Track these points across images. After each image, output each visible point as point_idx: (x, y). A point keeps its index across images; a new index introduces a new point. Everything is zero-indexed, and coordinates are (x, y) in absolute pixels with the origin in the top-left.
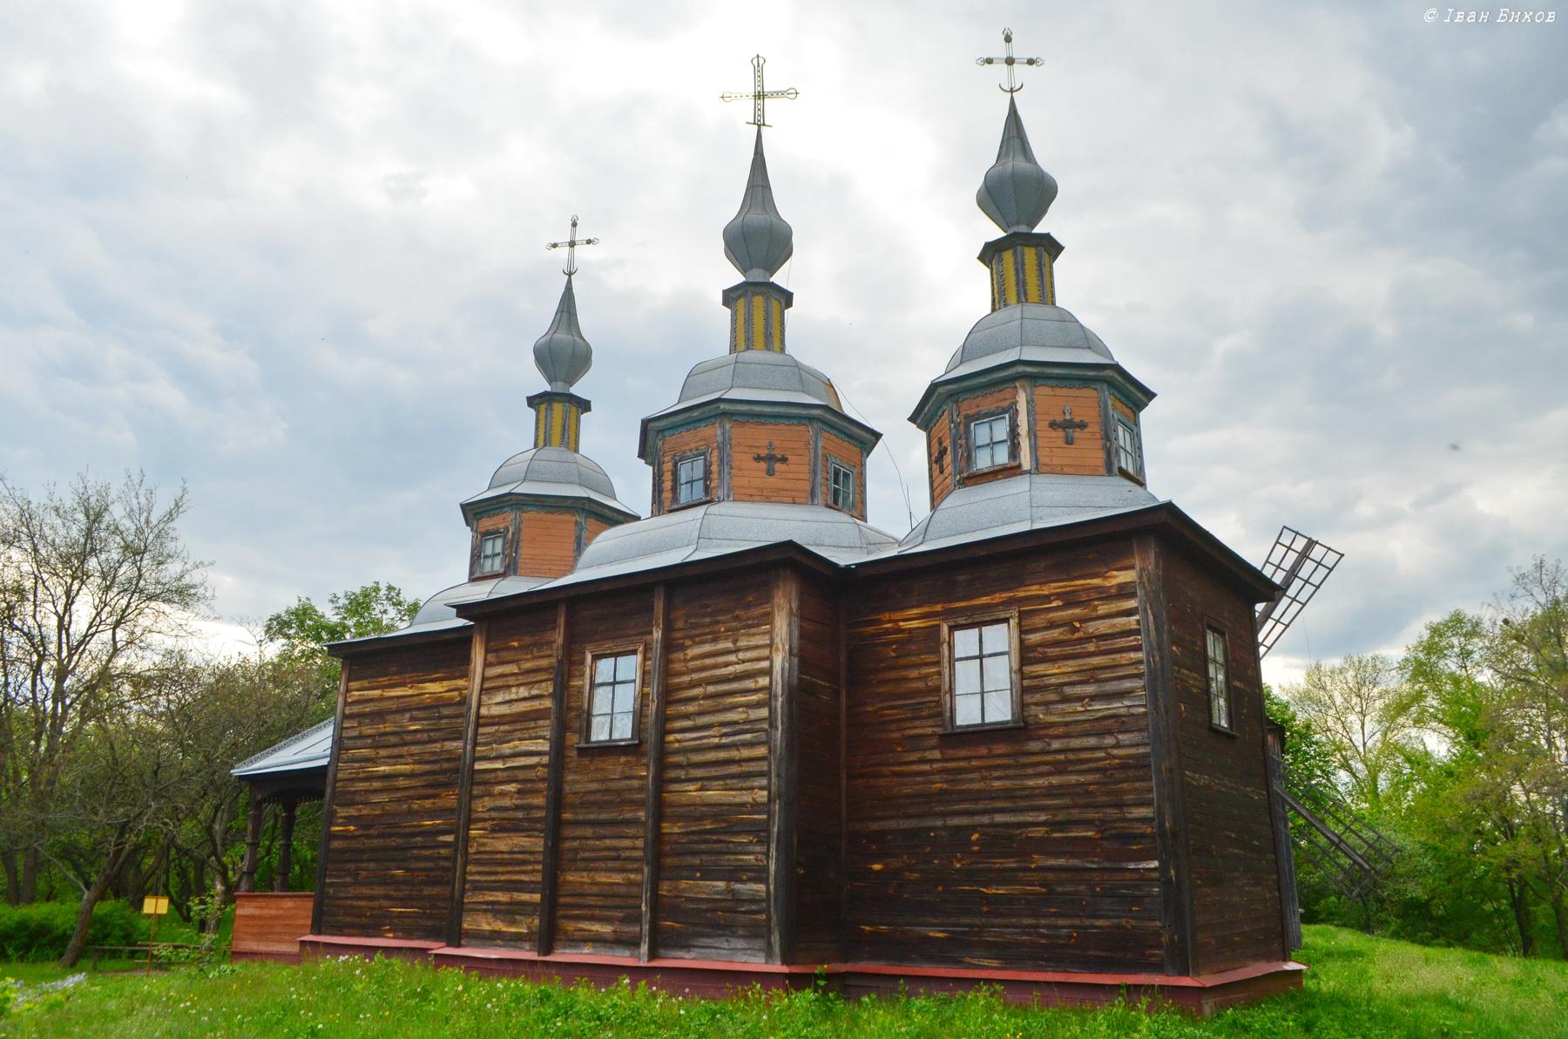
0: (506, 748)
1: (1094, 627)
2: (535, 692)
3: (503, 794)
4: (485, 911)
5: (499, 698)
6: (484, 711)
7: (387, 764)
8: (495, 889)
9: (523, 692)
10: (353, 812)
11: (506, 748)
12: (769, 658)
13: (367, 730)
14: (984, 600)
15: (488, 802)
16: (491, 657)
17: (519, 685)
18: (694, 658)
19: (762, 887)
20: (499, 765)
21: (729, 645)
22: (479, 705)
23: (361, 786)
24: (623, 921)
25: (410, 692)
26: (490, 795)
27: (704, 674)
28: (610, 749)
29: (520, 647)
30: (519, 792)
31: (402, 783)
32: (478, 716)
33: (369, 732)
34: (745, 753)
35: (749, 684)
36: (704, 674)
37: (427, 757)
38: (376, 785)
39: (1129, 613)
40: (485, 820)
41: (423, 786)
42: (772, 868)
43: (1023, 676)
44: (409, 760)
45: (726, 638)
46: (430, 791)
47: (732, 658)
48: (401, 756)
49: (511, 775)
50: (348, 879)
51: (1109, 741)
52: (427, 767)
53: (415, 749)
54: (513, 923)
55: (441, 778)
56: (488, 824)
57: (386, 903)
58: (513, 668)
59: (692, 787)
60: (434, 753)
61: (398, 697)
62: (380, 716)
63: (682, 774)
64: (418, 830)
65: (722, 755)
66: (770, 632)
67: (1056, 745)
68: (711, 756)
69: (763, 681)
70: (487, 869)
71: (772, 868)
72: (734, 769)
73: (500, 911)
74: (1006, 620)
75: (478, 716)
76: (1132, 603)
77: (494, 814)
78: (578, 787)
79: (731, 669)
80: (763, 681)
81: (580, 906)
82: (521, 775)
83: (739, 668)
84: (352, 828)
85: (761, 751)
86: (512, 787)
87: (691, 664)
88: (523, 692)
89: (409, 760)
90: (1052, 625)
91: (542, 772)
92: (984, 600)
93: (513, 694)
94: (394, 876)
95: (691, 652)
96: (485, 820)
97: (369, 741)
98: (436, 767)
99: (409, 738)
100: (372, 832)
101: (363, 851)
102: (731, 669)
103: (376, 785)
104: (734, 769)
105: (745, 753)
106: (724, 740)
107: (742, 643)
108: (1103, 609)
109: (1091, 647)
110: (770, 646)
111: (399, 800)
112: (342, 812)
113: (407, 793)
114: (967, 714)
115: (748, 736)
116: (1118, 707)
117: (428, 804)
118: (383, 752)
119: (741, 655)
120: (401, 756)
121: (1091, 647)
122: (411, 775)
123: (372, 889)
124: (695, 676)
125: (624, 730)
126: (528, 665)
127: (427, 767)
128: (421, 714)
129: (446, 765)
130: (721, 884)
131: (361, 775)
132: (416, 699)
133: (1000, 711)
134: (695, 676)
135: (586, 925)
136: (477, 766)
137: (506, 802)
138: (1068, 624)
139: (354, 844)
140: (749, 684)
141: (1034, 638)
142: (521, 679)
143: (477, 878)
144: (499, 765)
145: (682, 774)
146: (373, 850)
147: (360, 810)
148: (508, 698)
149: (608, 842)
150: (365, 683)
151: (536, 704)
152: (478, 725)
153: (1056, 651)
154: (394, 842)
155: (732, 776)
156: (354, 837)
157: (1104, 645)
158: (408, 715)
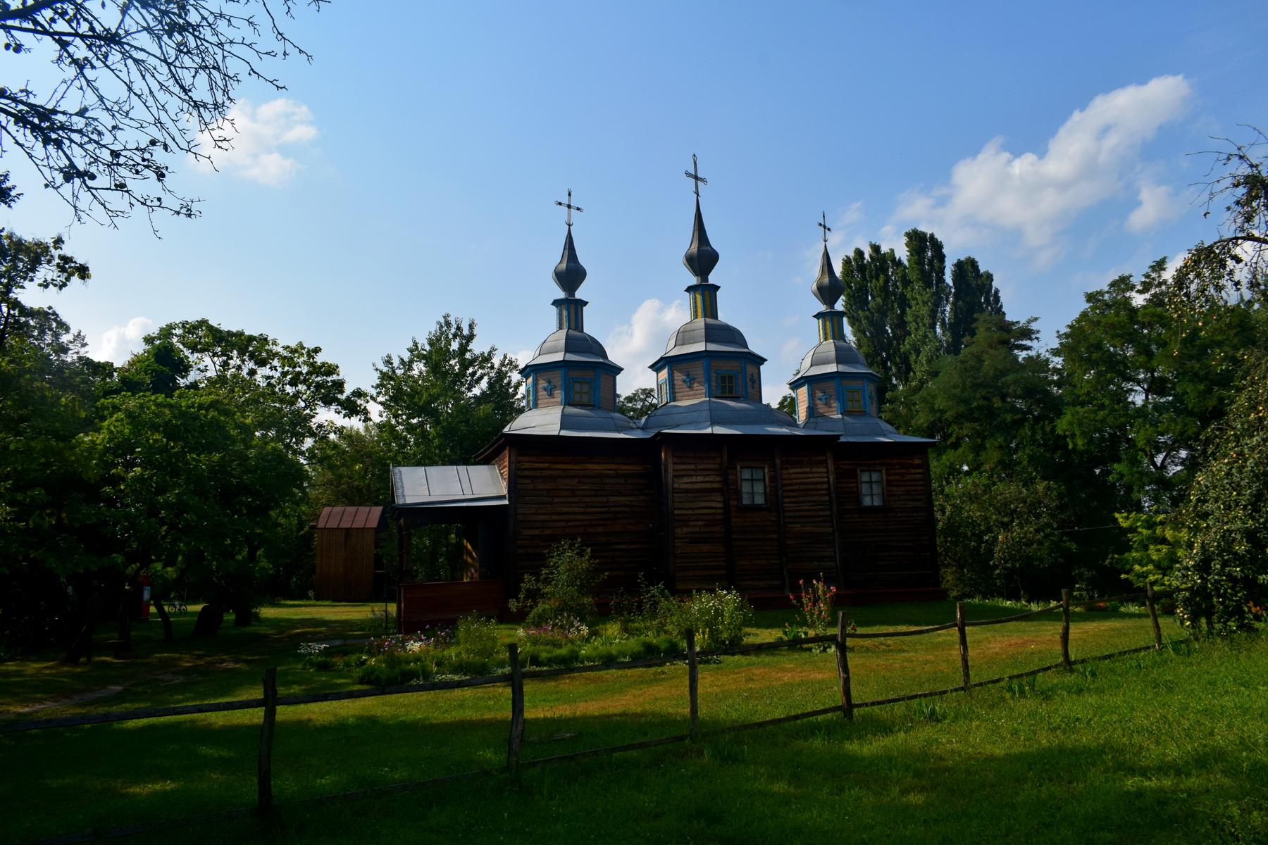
0: (694, 505)
1: (908, 477)
2: (706, 479)
3: (696, 526)
5: (686, 480)
6: (676, 486)
9: (699, 479)
10: (535, 532)
12: (828, 477)
15: (685, 530)
16: (676, 460)
17: (697, 475)
18: (793, 473)
19: (834, 564)
20: (691, 512)
21: (808, 470)
22: (673, 483)
25: (576, 467)
27: (798, 481)
28: (754, 508)
30: (704, 525)
32: (673, 489)
34: (821, 513)
35: (819, 486)
36: (798, 481)
38: (554, 517)
39: (920, 473)
40: (684, 538)
42: (838, 557)
44: (582, 505)
45: (807, 467)
47: (811, 475)
51: (916, 514)
52: (598, 510)
58: (692, 467)
59: (798, 526)
61: (565, 470)
63: (792, 520)
65: (812, 513)
66: (827, 467)
68: (806, 513)
71: (838, 557)
72: (817, 519)
74: (881, 471)
75: (673, 489)
76: (921, 471)
79: (810, 480)
80: (825, 486)
83: (814, 480)
85: (828, 513)
86: (701, 523)
87: (792, 476)
88: (699, 479)
89: (582, 505)
90: (896, 474)
91: (718, 517)
93: (694, 479)
95: (791, 471)
96: (684, 538)
98: (605, 510)
102: (810, 480)
103: (554, 517)
104: (817, 519)
105: (821, 513)
106: (812, 508)
107: (814, 470)
108: (913, 471)
109: (909, 483)
110: (828, 472)
114: (867, 501)
115: (822, 507)
116: (918, 504)
117: (600, 529)
118: (557, 500)
119: (815, 475)
121: (909, 483)
122: (584, 513)
124: (795, 481)
125: (759, 500)
126: (701, 467)
127: (598, 510)
129: (612, 509)
130: (816, 563)
132: (582, 472)
133: (877, 502)
134: (795, 481)
136: (676, 512)
137: (697, 529)
140: (819, 486)
141: (890, 478)
144: (691, 512)
145: (792, 520)
148: (690, 480)
151: (708, 486)
152: (673, 492)
153: (895, 483)
157: (913, 483)
158: (577, 480)
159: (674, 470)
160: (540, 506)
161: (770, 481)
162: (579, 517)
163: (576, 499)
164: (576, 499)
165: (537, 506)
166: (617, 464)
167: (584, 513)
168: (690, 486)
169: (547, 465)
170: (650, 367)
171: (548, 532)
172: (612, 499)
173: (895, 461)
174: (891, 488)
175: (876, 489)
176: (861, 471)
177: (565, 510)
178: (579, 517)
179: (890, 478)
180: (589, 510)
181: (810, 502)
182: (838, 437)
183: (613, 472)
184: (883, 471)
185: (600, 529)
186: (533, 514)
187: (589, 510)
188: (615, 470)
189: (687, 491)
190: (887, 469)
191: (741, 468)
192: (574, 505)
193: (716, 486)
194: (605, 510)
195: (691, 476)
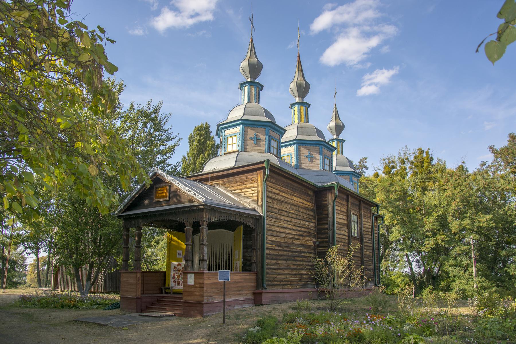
33: (276, 207)
41: (297, 235)
46: (298, 237)
53: (293, 220)
55: (301, 233)
57: (289, 276)
60: (299, 224)
64: (295, 250)
84: (274, 246)
89: (291, 224)
98: (299, 229)
99: (291, 215)
100: (281, 248)
106: (368, 241)
113: (291, 236)
117: (298, 242)
118: (282, 218)
123: (284, 271)
146: (282, 255)
147: (276, 239)
158: (289, 206)
160: (276, 220)
161: (360, 224)
162: (291, 232)
163: (289, 219)
164: (289, 219)
165: (274, 220)
166: (303, 199)
167: (292, 230)
169: (277, 192)
171: (278, 240)
177: (286, 226)
178: (291, 232)
180: (295, 228)
183: (301, 204)
185: (298, 242)
186: (272, 225)
187: (295, 228)
188: (303, 203)
192: (289, 223)
193: (346, 222)
194: (299, 229)
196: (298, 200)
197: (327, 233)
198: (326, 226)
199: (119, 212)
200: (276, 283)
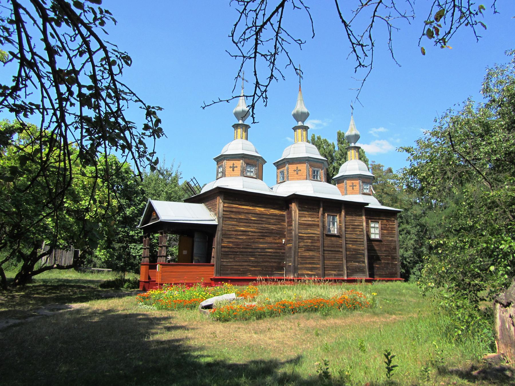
2: (313, 219)
3: (307, 242)
4: (304, 269)
5: (303, 219)
7: (243, 228)
8: (306, 264)
9: (310, 219)
11: (306, 231)
13: (233, 216)
14: (375, 218)
17: (308, 217)
23: (233, 233)
24: (339, 271)
26: (304, 242)
29: (307, 208)
30: (312, 242)
31: (250, 234)
33: (234, 217)
37: (260, 228)
38: (239, 233)
40: (302, 248)
41: (259, 236)
43: (381, 232)
48: (250, 226)
49: (309, 238)
50: (231, 260)
54: (312, 271)
56: (303, 249)
57: (248, 267)
60: (263, 227)
62: (239, 213)
65: (355, 240)
67: (385, 243)
69: (362, 227)
70: (304, 259)
73: (309, 269)
74: (378, 222)
75: (299, 223)
77: (304, 247)
78: (327, 243)
81: (328, 268)
82: (311, 238)
84: (231, 245)
86: (310, 241)
88: (310, 219)
92: (375, 218)
94: (249, 260)
97: (236, 220)
99: (252, 221)
101: (237, 252)
103: (239, 233)
106: (356, 237)
111: (250, 239)
112: (225, 240)
120: (250, 226)
122: (254, 232)
127: (261, 231)
128: (256, 215)
130: (357, 264)
131: (233, 230)
133: (377, 237)
135: (330, 272)
137: (308, 244)
138: (386, 225)
139: (232, 250)
142: (309, 216)
143: (301, 261)
146: (241, 252)
148: (306, 219)
149: (333, 255)
150: (231, 202)
151: (314, 223)
154: (250, 250)
155: (358, 244)
156: (232, 248)
158: (251, 215)
159: (299, 214)
168: (305, 222)
170: (274, 164)
172: (267, 226)
173: (384, 218)
174: (383, 231)
175: (377, 231)
176: (371, 221)
179: (382, 226)
180: (256, 230)
181: (355, 234)
182: (367, 204)
184: (380, 222)
189: (304, 224)
190: (381, 222)
191: (328, 215)
195: (305, 217)
196: (262, 209)
197: (291, 233)
198: (291, 228)
199: (140, 226)
200: (233, 272)
